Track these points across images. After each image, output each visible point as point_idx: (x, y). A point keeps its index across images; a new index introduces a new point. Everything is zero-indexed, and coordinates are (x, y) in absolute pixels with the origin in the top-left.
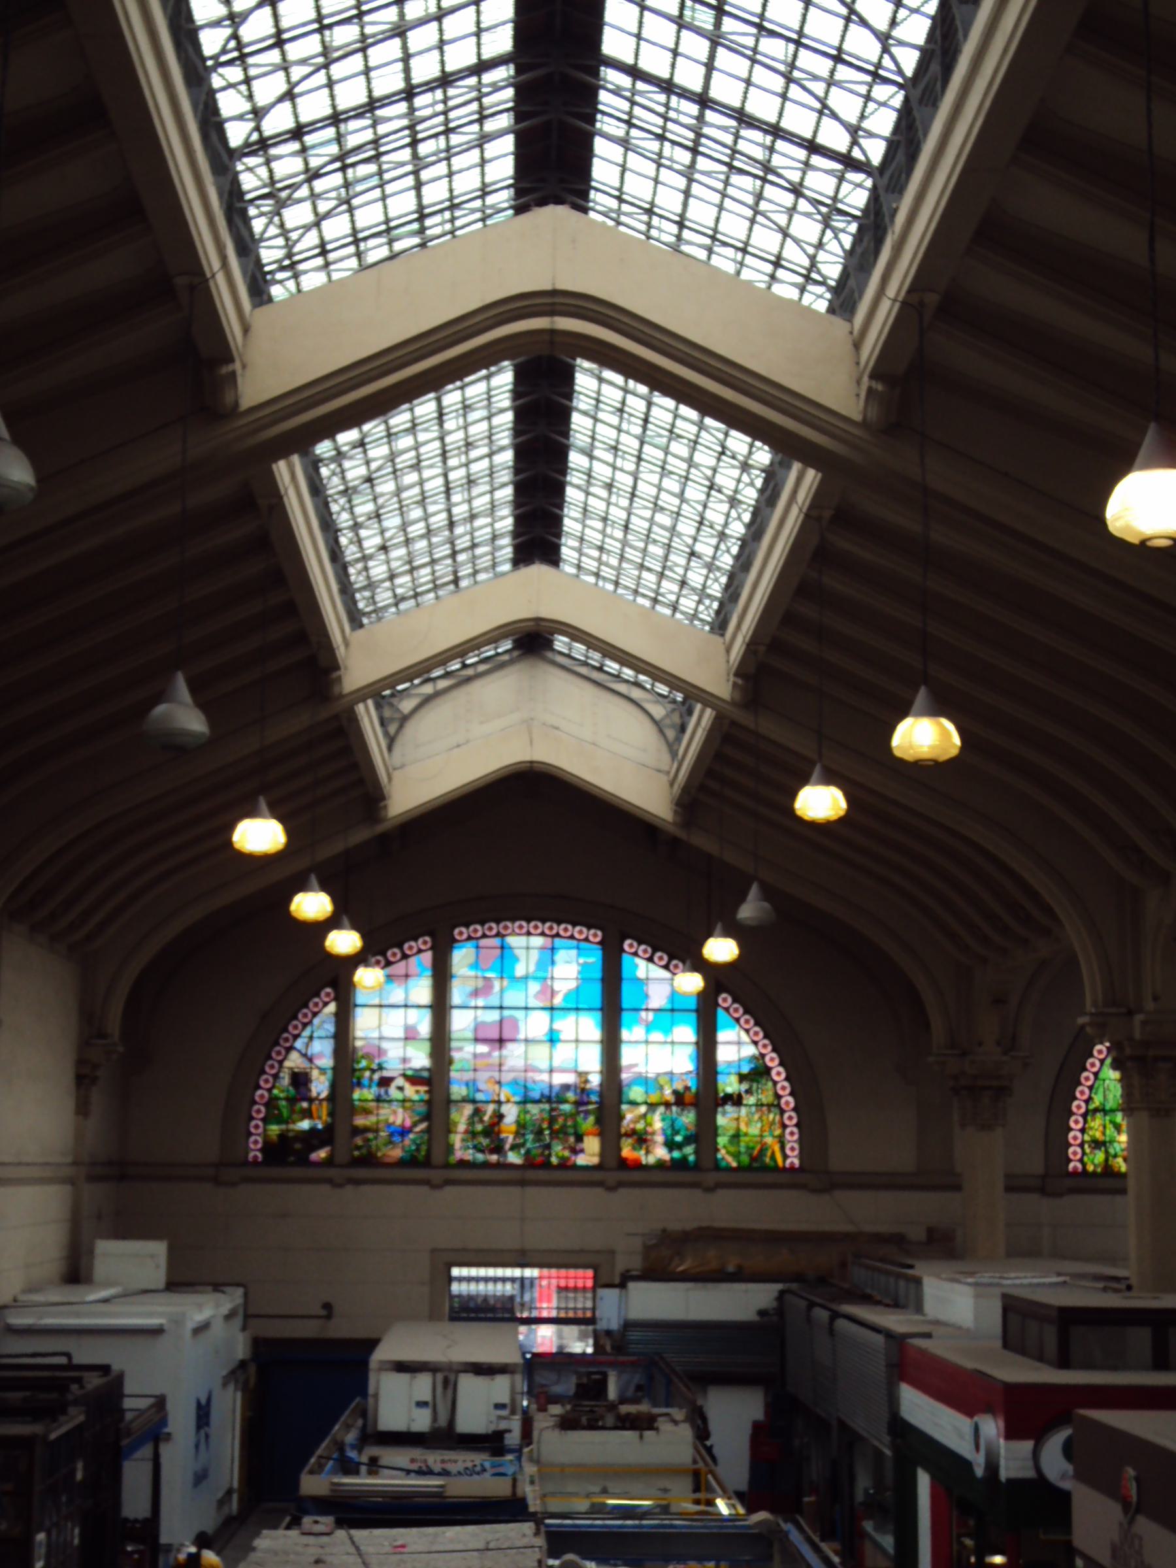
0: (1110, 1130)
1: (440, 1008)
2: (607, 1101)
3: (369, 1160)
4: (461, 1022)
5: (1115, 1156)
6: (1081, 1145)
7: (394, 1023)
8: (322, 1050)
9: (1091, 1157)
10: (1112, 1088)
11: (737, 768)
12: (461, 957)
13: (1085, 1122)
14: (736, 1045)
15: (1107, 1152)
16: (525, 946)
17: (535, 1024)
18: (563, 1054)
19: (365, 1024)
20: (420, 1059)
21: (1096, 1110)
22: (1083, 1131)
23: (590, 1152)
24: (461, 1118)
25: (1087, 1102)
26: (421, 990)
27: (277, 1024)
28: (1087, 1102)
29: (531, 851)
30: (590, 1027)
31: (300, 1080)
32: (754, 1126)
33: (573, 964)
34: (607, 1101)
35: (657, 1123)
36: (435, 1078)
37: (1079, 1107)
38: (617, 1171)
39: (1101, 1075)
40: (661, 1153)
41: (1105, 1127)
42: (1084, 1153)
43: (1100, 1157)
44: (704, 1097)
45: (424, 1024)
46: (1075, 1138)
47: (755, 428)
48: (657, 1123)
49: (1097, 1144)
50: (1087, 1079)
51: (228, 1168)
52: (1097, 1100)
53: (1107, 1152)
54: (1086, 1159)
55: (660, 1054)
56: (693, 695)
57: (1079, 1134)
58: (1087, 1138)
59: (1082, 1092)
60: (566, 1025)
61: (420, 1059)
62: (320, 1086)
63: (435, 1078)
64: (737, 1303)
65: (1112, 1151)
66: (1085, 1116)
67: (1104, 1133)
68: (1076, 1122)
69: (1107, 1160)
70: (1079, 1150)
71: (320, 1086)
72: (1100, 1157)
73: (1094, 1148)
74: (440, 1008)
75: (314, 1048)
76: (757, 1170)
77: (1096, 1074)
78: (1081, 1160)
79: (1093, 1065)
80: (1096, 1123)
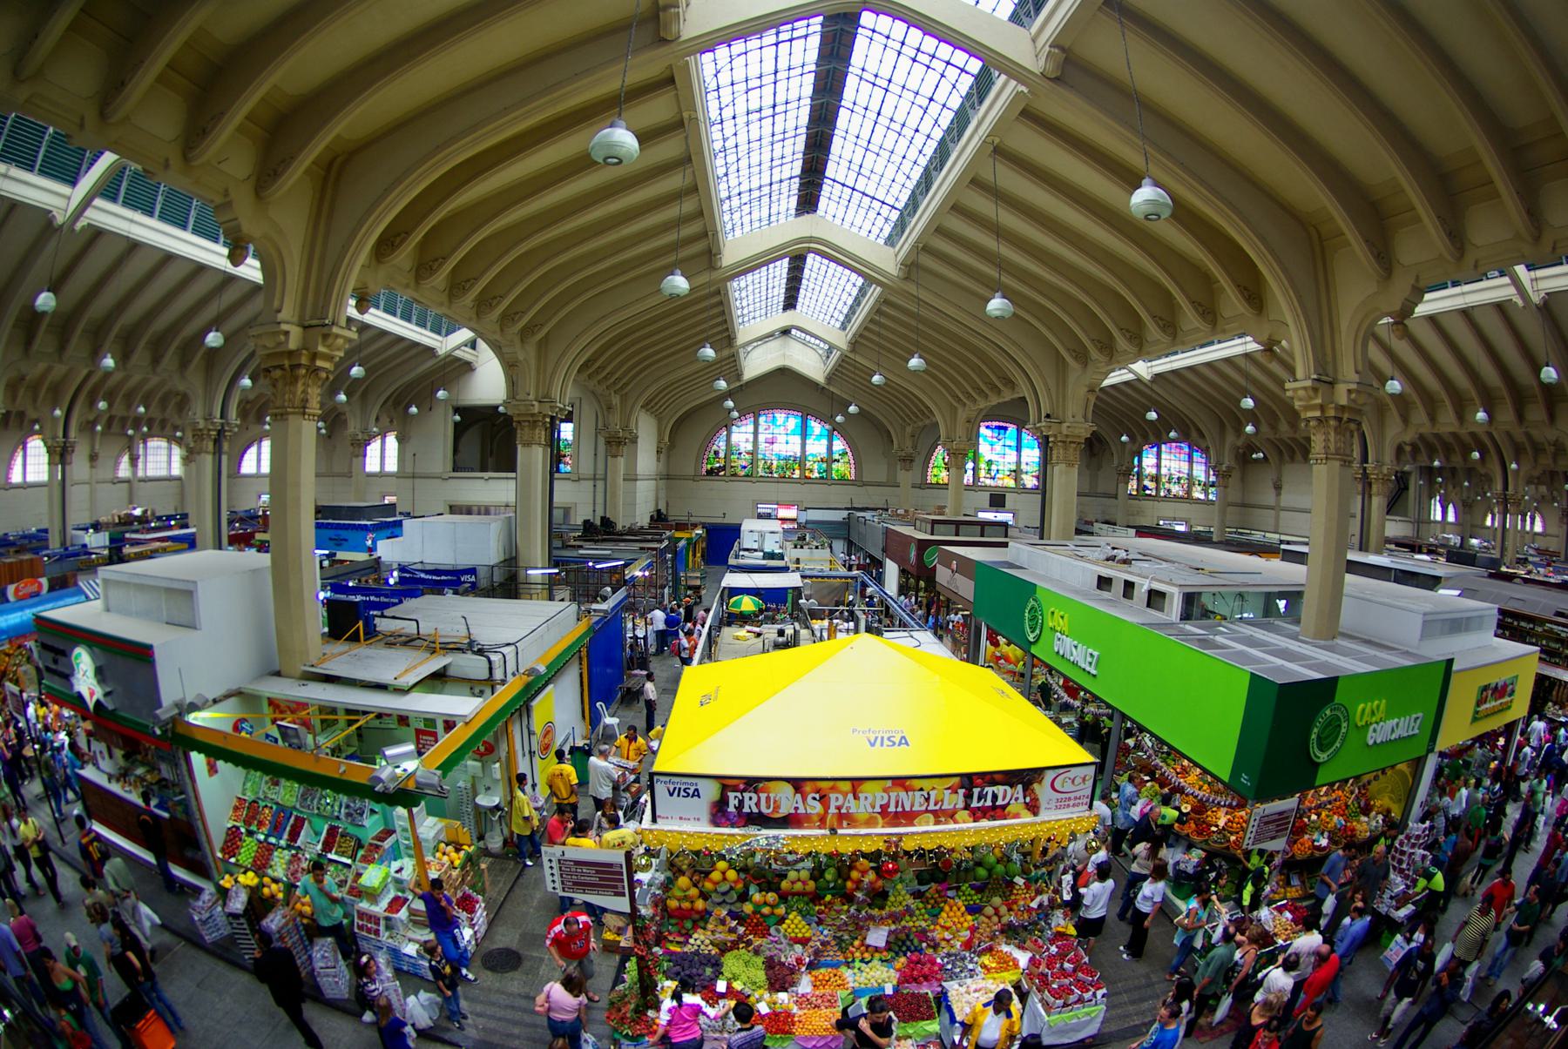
1: (756, 433)
2: (802, 460)
3: (735, 475)
4: (761, 438)
7: (743, 437)
8: (722, 445)
11: (845, 369)
12: (762, 419)
14: (839, 445)
16: (780, 416)
17: (782, 439)
18: (789, 447)
19: (735, 438)
20: (750, 447)
23: (797, 474)
24: (761, 464)
26: (750, 428)
27: (710, 438)
29: (784, 389)
30: (798, 439)
31: (716, 453)
32: (843, 468)
33: (794, 422)
34: (802, 460)
35: (816, 466)
36: (754, 453)
38: (805, 479)
40: (816, 475)
44: (829, 460)
45: (751, 437)
47: (860, 273)
48: (816, 466)
51: (695, 478)
55: (817, 448)
56: (832, 347)
60: (790, 438)
61: (750, 447)
62: (722, 455)
63: (754, 453)
64: (839, 516)
71: (722, 455)
74: (756, 433)
75: (720, 444)
76: (843, 481)
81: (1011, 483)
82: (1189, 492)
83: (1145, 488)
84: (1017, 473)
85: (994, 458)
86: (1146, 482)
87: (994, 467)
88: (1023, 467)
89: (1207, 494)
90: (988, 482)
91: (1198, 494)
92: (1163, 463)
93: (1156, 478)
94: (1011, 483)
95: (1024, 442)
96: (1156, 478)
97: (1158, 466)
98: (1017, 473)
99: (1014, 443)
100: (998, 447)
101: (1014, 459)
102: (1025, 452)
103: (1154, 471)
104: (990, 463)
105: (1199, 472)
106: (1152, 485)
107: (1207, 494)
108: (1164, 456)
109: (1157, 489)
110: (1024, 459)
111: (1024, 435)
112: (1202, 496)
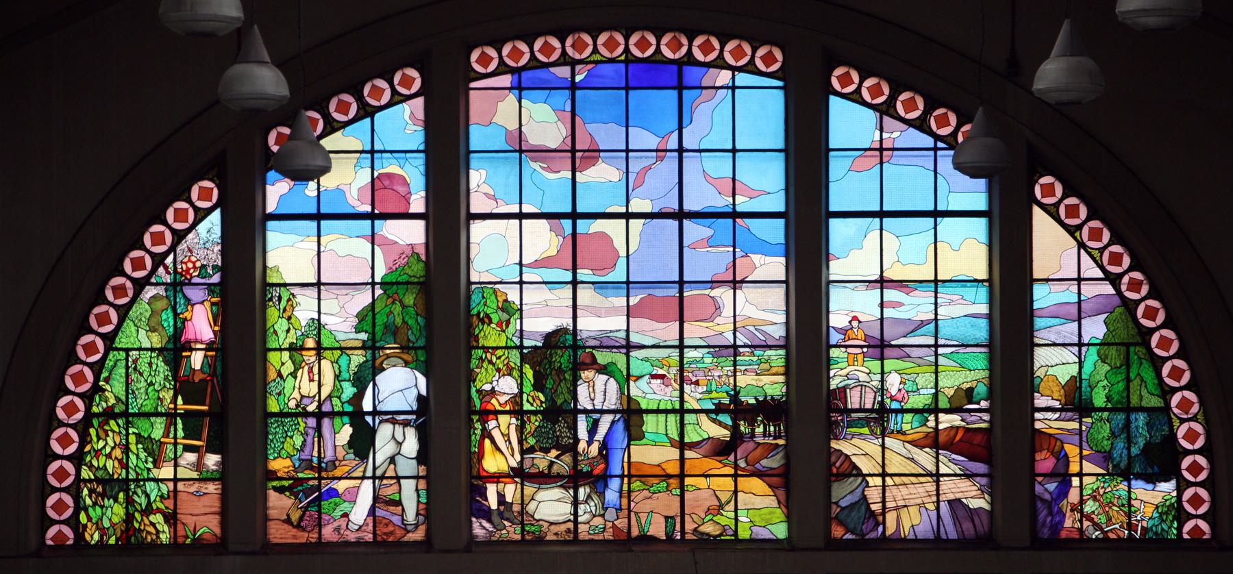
0: (138, 459)
5: (148, 510)
6: (74, 490)
9: (95, 513)
10: (143, 367)
13: (84, 439)
15: (129, 501)
21: (109, 414)
22: (77, 459)
25: (88, 397)
28: (88, 397)
37: (70, 409)
39: (122, 341)
41: (126, 449)
42: (79, 507)
43: (116, 512)
46: (61, 474)
49: (109, 486)
50: (90, 349)
52: (115, 389)
53: (129, 501)
54: (83, 518)
57: (69, 467)
58: (86, 473)
59: (78, 377)
65: (143, 501)
66: (83, 428)
67: (125, 466)
68: (65, 441)
69: (129, 518)
70: (68, 500)
72: (116, 512)
73: (103, 495)
77: (109, 339)
78: (73, 522)
79: (103, 319)
80: (106, 442)
81: (759, 512)
84: (799, 423)
85: (601, 318)
87: (595, 391)
88: (849, 372)
90: (551, 506)
94: (759, 512)
95: (847, 186)
98: (799, 423)
99: (766, 184)
100: (641, 248)
101: (764, 309)
102: (852, 253)
104: (560, 358)
110: (847, 307)
111: (849, 123)
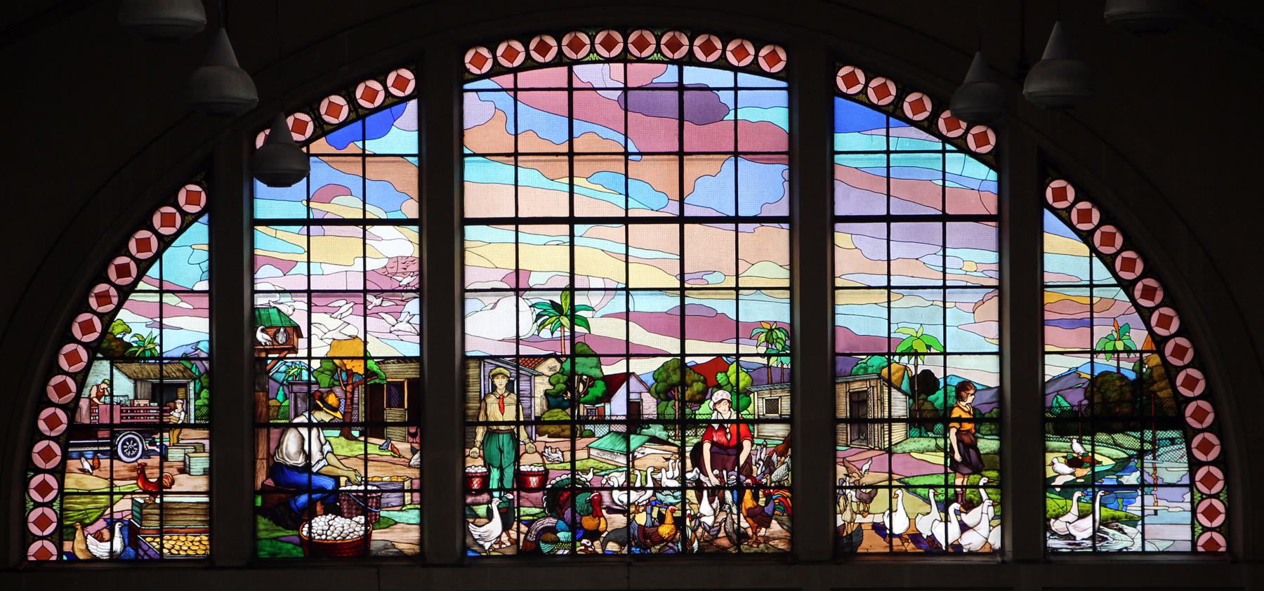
82: (813, 488)
83: (297, 493)
86: (314, 446)
89: (1025, 502)
91: (908, 501)
92: (485, 255)
93: (433, 397)
96: (433, 397)
97: (440, 287)
103: (396, 337)
105: (923, 294)
106: (392, 461)
107: (1025, 502)
108: (485, 188)
109: (445, 496)
112: (981, 530)
